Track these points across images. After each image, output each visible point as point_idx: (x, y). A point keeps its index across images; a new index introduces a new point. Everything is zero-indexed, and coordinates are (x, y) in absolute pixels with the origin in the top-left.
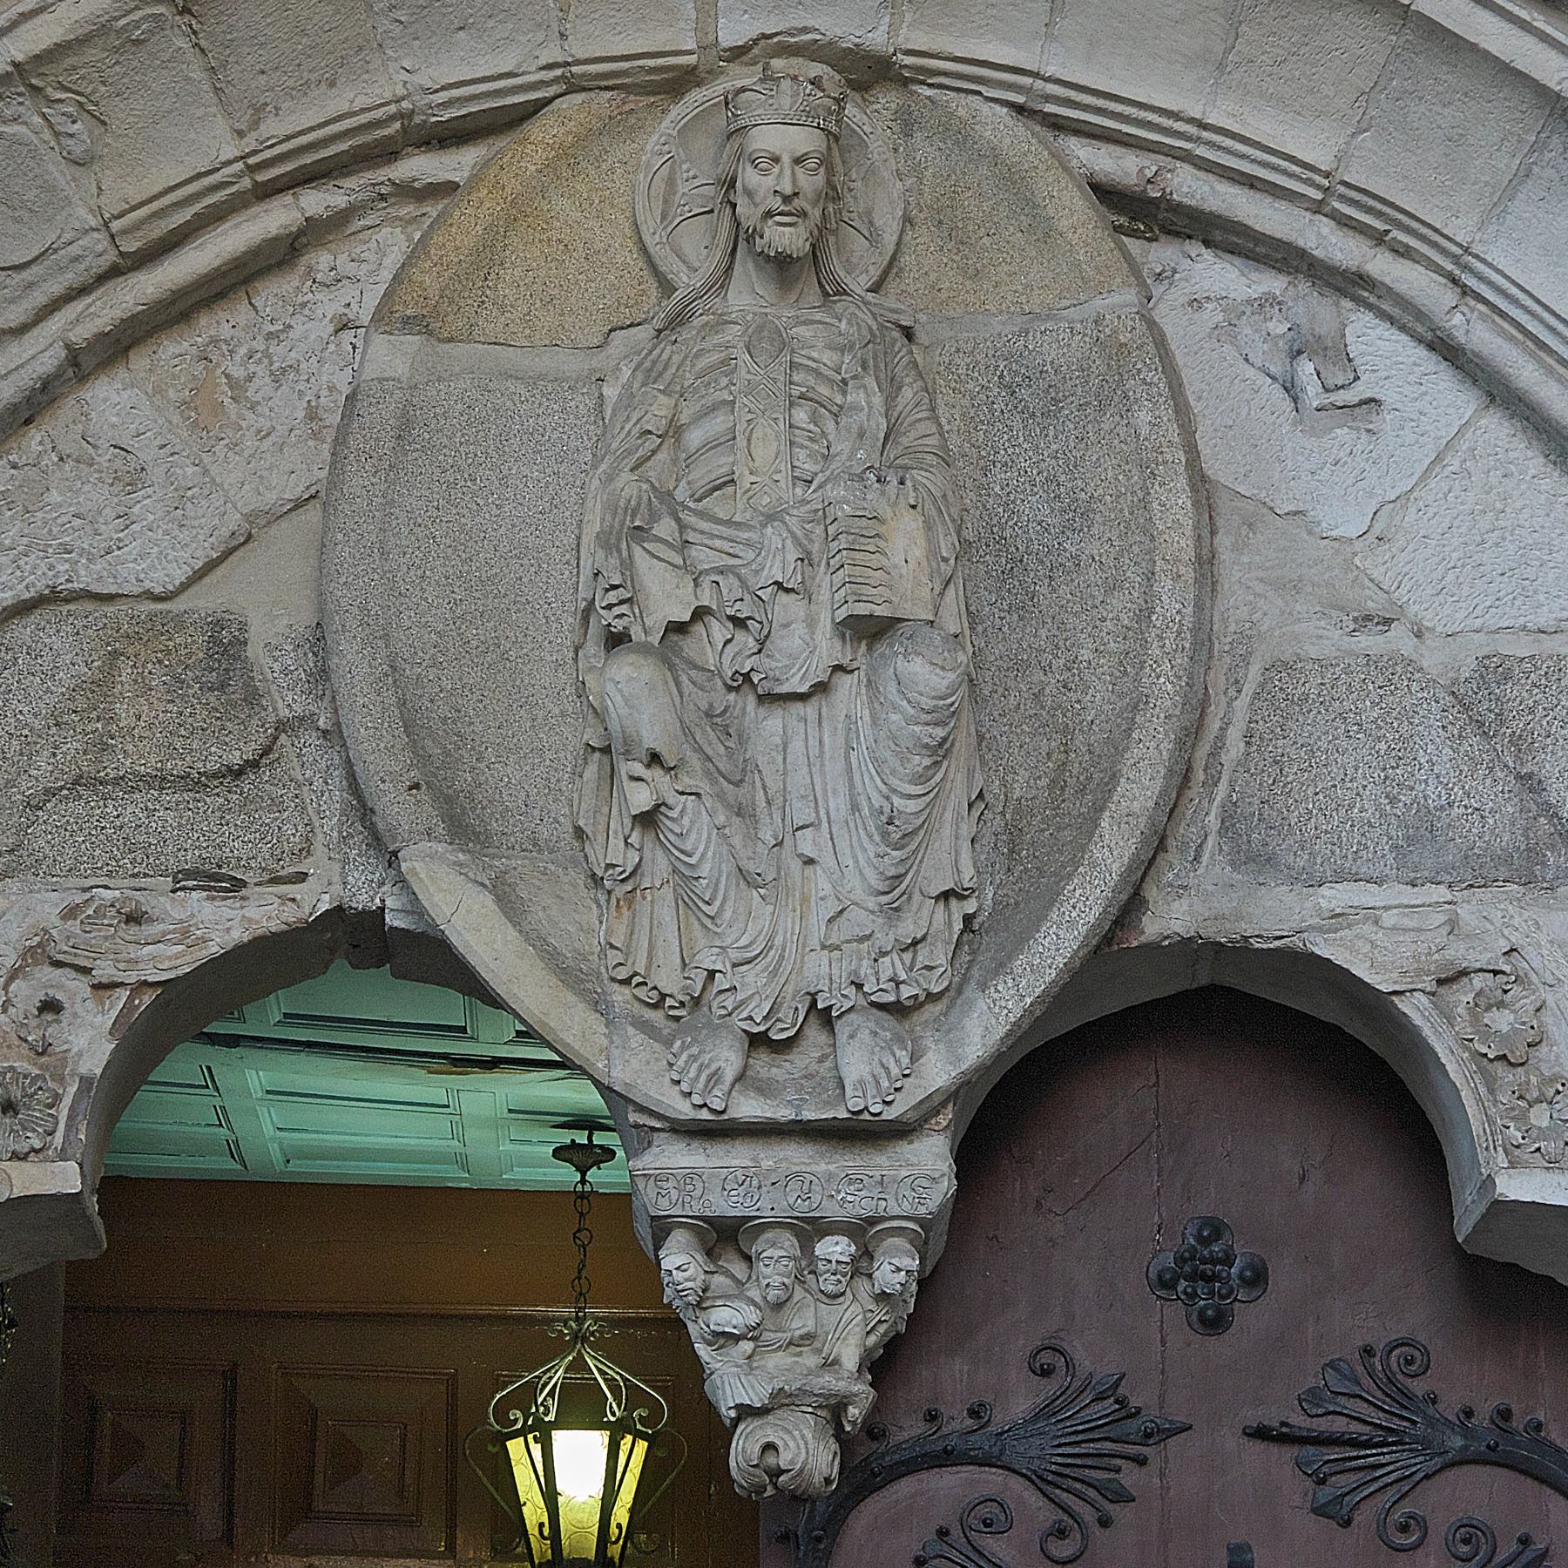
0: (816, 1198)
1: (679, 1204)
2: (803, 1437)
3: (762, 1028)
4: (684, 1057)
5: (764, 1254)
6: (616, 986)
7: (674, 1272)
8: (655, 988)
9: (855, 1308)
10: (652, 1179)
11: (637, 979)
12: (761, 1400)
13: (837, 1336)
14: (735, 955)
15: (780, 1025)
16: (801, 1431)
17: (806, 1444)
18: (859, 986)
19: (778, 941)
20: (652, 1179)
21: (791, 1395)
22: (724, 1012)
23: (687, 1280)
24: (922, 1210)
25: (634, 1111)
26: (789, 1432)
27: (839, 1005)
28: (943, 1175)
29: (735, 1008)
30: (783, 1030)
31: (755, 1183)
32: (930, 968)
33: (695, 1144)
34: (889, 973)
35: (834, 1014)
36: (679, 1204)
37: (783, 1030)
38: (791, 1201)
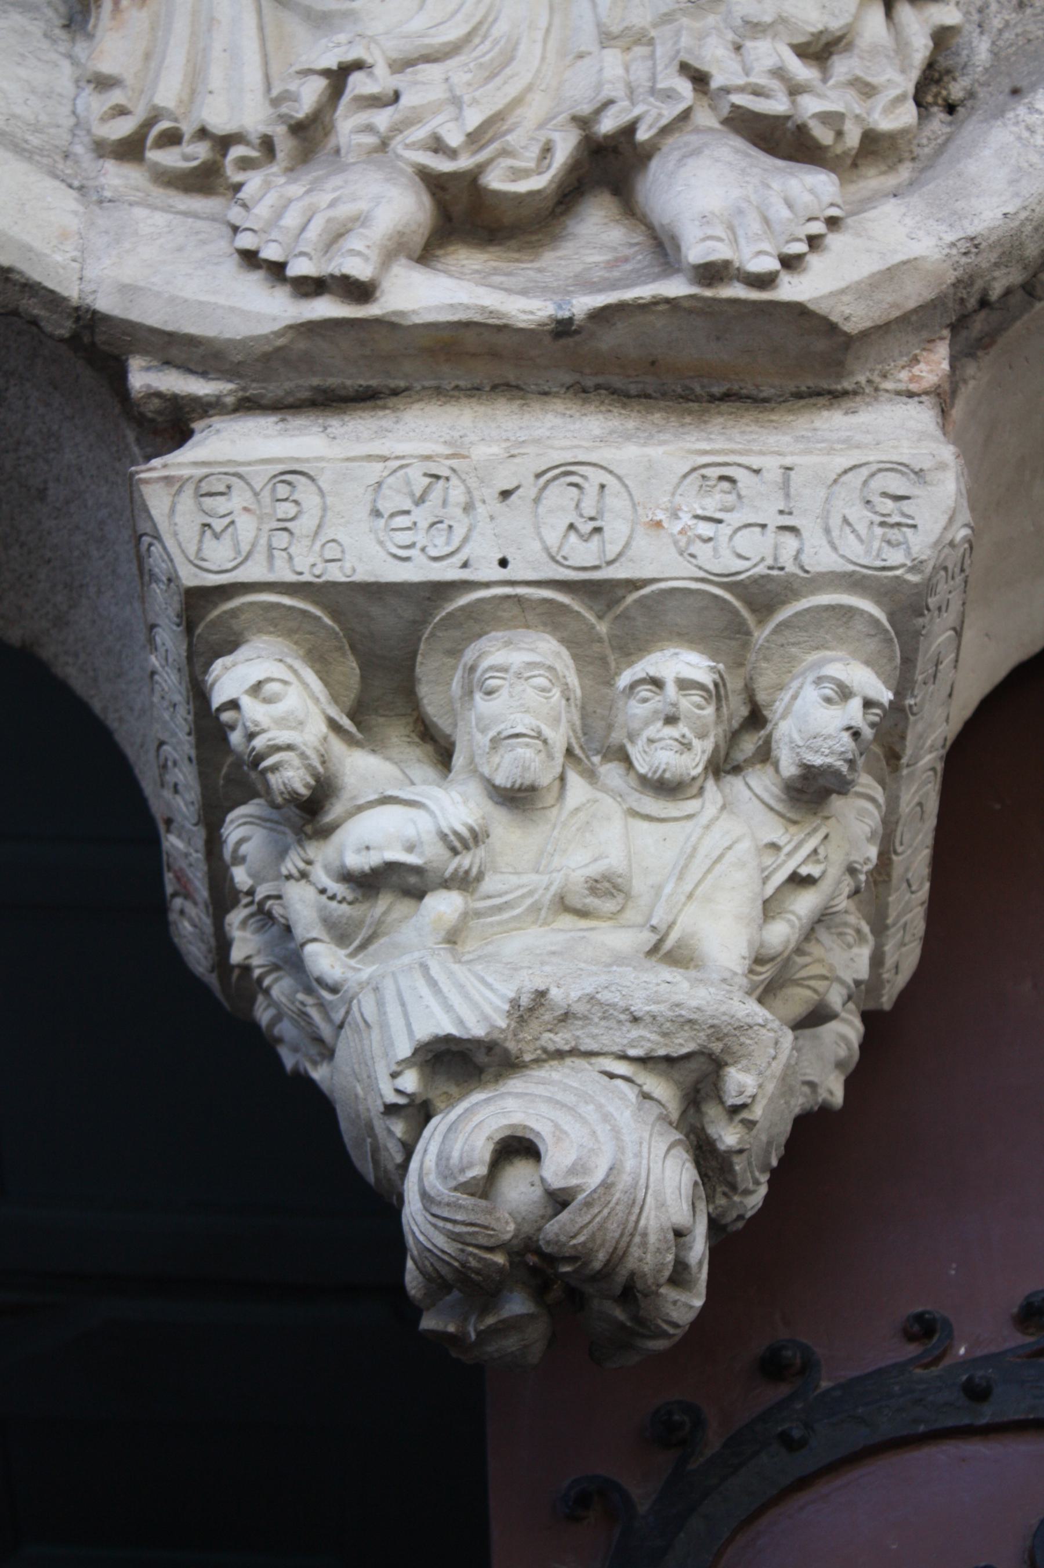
0: (616, 531)
1: (260, 556)
2: (606, 1118)
3: (464, 163)
4: (271, 198)
5: (485, 664)
6: (110, 166)
7: (246, 702)
8: (203, 133)
9: (728, 828)
10: (189, 491)
11: (164, 125)
12: (486, 1018)
13: (688, 887)
14: (396, 47)
15: (506, 162)
16: (600, 1107)
17: (616, 1133)
18: (699, 79)
19: (501, 28)
20: (189, 491)
21: (566, 1017)
22: (370, 140)
23: (282, 722)
24: (895, 557)
25: (148, 369)
26: (563, 1105)
27: (654, 112)
28: (942, 466)
29: (397, 129)
30: (518, 174)
31: (457, 494)
32: (867, 90)
33: (298, 422)
34: (770, 62)
35: (643, 135)
36: (260, 556)
37: (518, 174)
38: (553, 538)
